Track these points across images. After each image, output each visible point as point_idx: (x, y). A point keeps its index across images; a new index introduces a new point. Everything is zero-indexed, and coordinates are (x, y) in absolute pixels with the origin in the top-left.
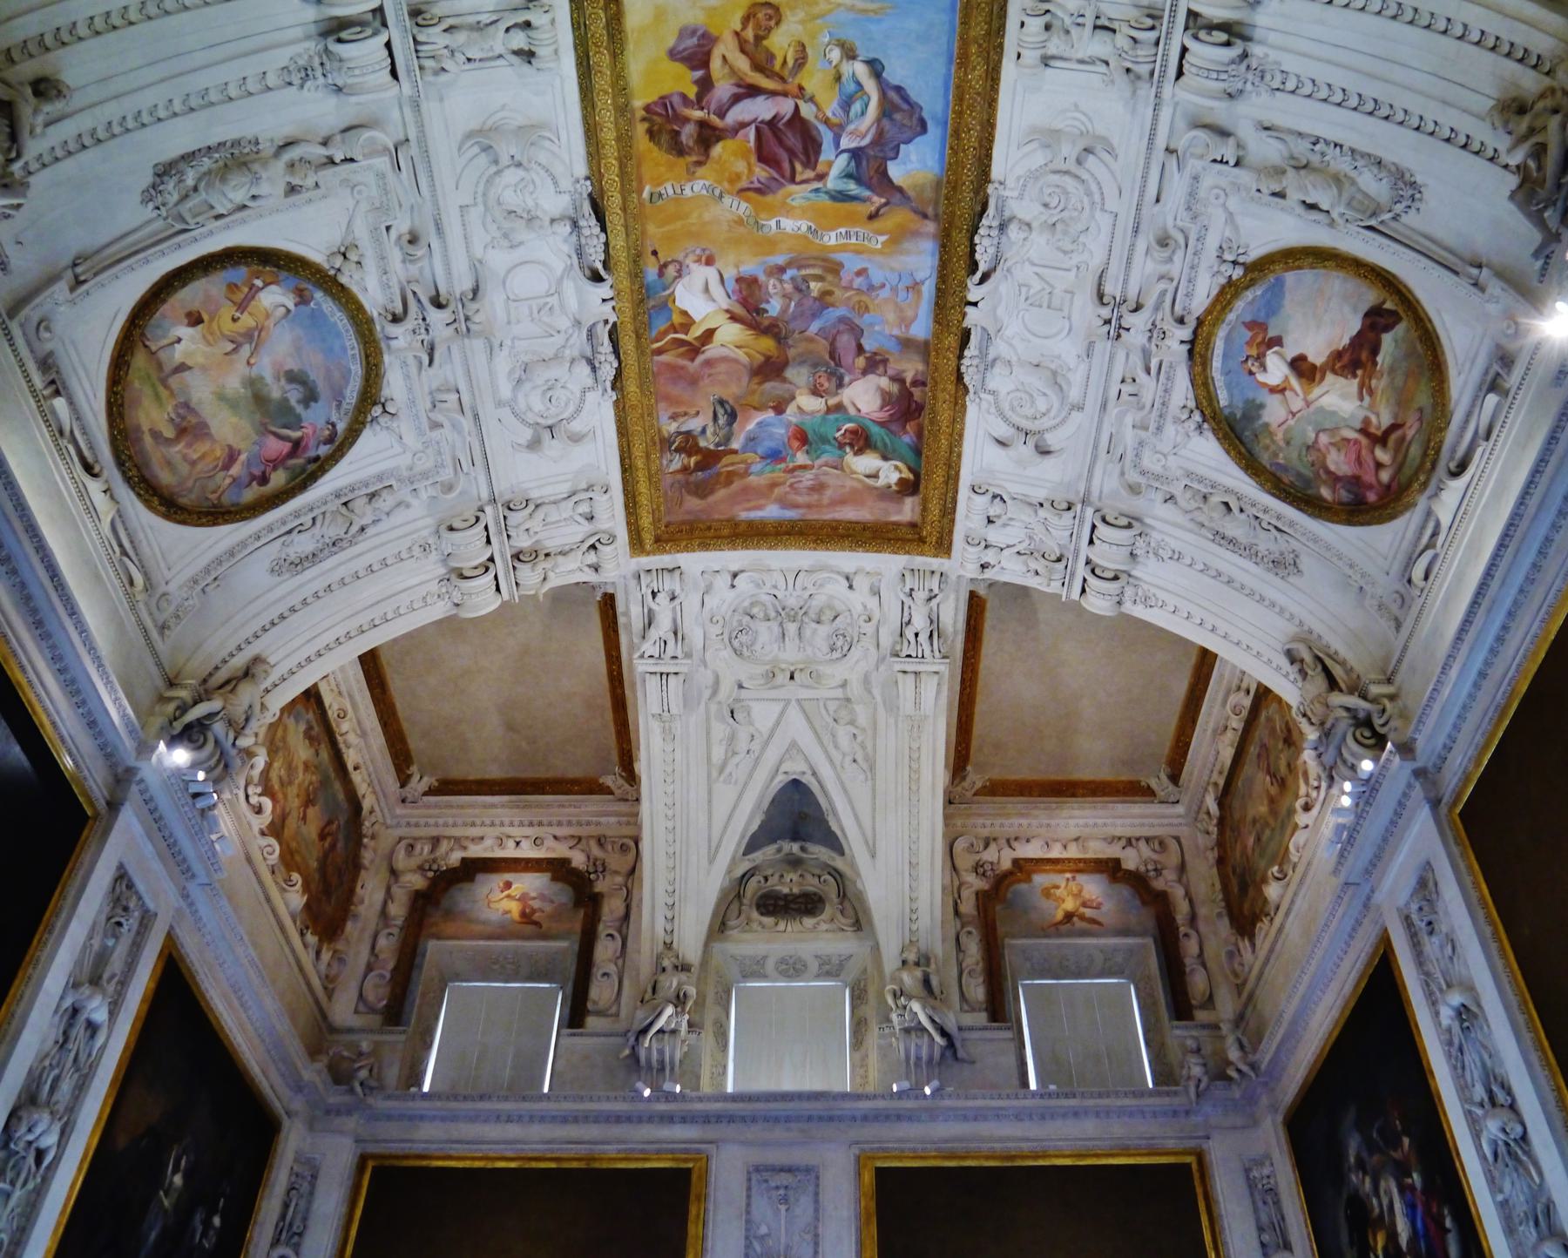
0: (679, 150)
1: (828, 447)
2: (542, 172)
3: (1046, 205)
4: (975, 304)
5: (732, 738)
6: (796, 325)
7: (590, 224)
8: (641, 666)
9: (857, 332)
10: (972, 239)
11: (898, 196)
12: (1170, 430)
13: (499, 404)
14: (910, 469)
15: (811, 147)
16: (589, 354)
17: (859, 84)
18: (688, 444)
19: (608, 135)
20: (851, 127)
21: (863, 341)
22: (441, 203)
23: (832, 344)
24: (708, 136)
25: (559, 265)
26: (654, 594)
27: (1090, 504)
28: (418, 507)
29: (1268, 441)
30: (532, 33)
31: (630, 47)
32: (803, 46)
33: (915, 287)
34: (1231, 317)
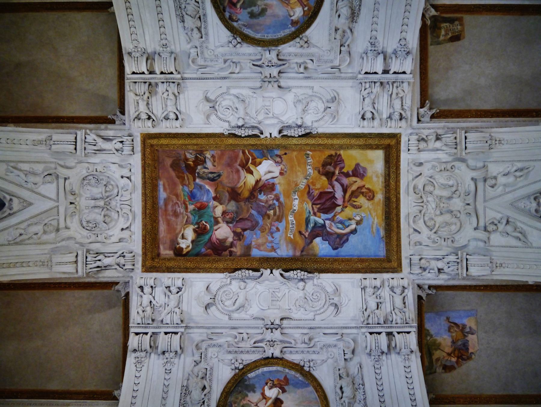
0: (324, 165)
1: (197, 218)
2: (321, 117)
3: (312, 295)
4: (272, 272)
5: (34, 174)
6: (254, 205)
7: (301, 132)
8: (80, 134)
9: (252, 228)
10: (298, 269)
11: (309, 241)
12: (230, 357)
13: (228, 88)
14: (188, 252)
15: (325, 210)
16: (246, 126)
17: (348, 226)
18: (200, 161)
19: (336, 142)
20: (333, 224)
23: (247, 219)
24: (329, 175)
25: (284, 119)
26: (122, 142)
27: (185, 329)
28: (186, 47)
29: (240, 398)
30: (371, 119)
31: (361, 151)
32: (361, 208)
33: (273, 249)
34: (287, 370)
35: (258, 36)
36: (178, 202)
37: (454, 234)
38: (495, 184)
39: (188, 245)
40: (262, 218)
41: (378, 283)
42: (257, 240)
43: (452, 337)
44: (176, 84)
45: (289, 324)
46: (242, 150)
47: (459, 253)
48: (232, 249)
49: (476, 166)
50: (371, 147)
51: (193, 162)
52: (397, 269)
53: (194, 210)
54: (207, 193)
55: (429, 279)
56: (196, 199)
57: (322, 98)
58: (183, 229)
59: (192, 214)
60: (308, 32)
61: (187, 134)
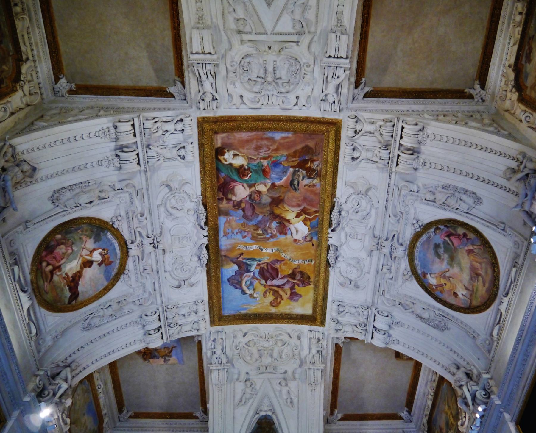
0: (302, 273)
1: (254, 168)
2: (343, 274)
4: (205, 236)
6: (267, 218)
7: (331, 261)
9: (245, 217)
10: (209, 256)
11: (234, 261)
13: (377, 208)
14: (220, 161)
17: (248, 288)
18: (310, 173)
19: (321, 286)
20: (250, 278)
21: (243, 213)
24: (293, 276)
25: (344, 247)
31: (312, 299)
33: (226, 234)
36: (271, 151)
37: (243, 358)
38: (281, 385)
39: (228, 160)
40: (254, 224)
41: (201, 313)
42: (235, 221)
43: (161, 349)
45: (159, 254)
46: (319, 211)
47: (229, 365)
48: (225, 200)
49: (295, 373)
50: (315, 306)
51: (310, 167)
52: (213, 323)
53: (262, 166)
54: (279, 178)
55: (206, 344)
56: (273, 167)
57: (360, 278)
58: (243, 155)
59: (258, 163)
61: (338, 165)
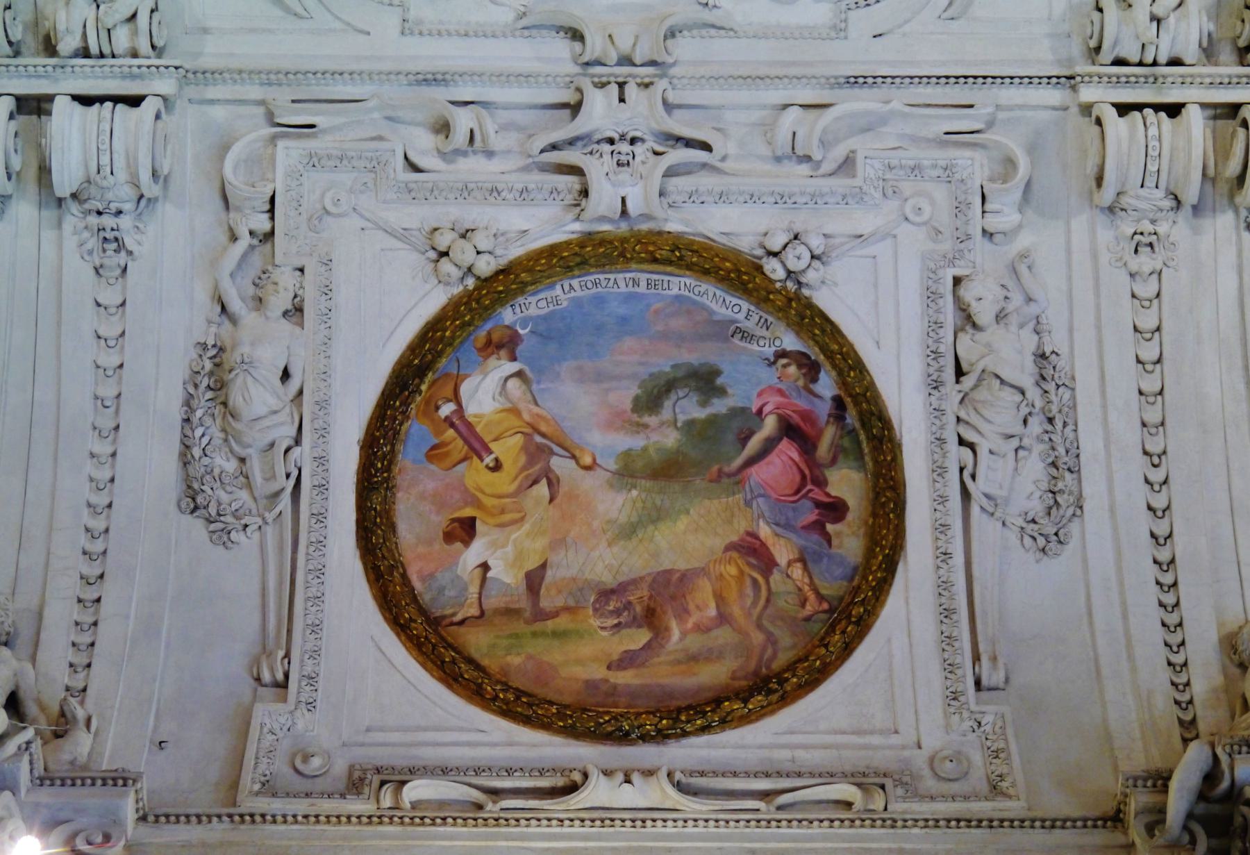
13: (839, 30)
22: (387, 66)
35: (680, 284)
44: (1106, 55)
60: (434, 301)
